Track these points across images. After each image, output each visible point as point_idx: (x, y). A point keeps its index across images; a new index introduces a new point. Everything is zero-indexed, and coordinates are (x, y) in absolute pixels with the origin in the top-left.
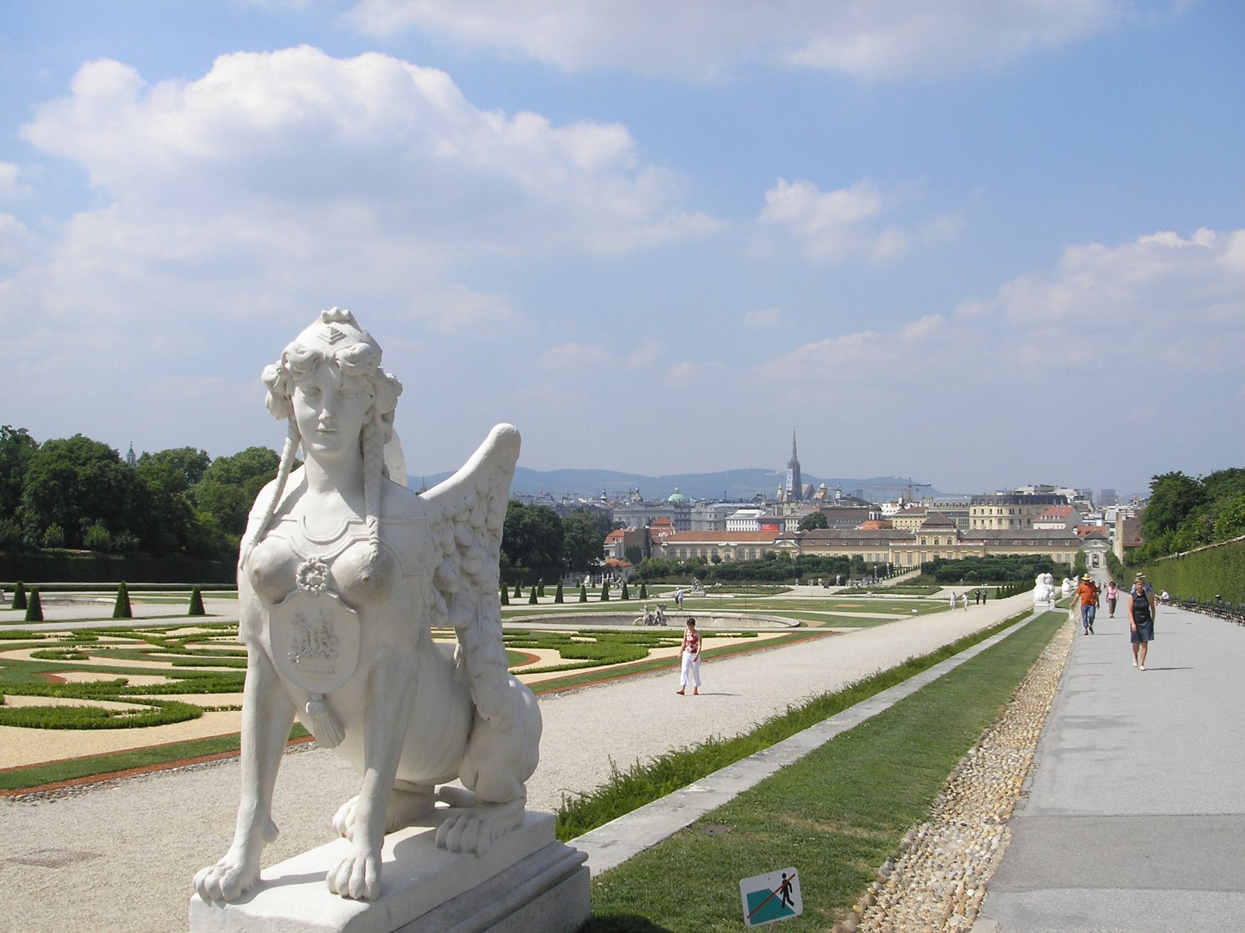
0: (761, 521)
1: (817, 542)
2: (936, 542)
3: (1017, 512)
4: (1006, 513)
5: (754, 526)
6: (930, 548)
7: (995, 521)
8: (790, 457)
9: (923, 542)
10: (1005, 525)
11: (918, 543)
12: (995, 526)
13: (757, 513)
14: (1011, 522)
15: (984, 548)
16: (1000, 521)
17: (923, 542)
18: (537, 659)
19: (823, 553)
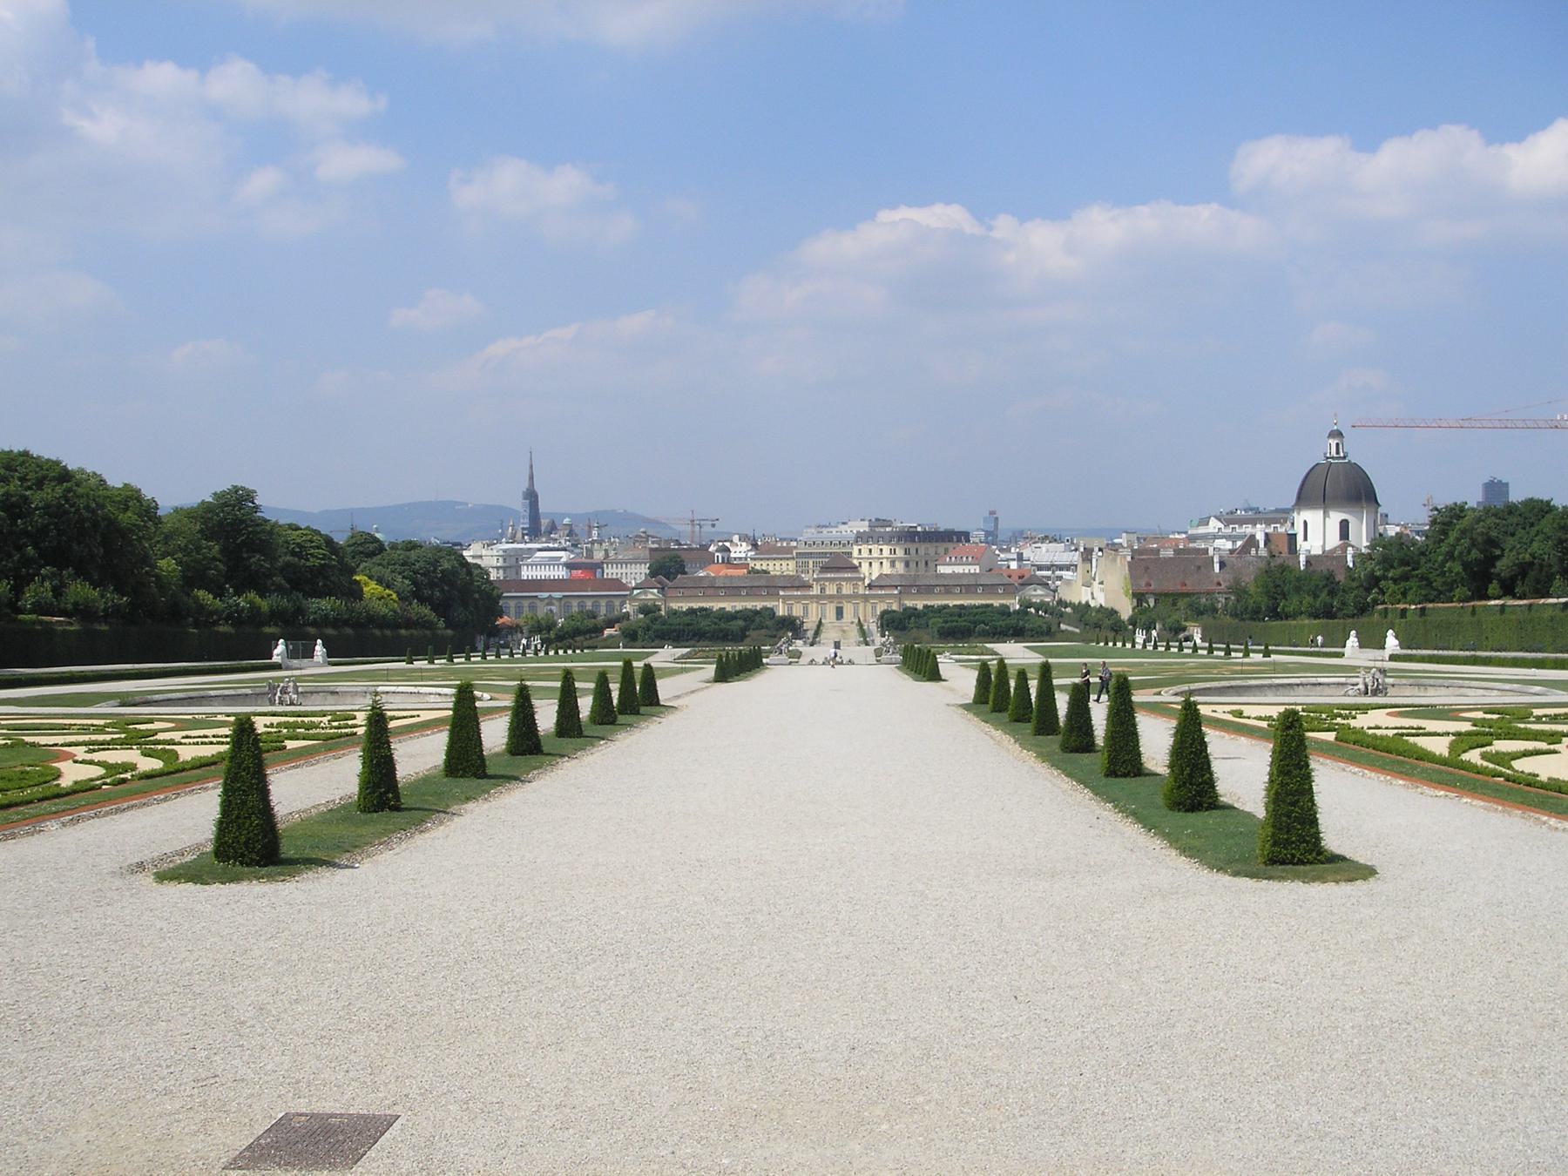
0: (570, 566)
1: (687, 592)
2: (839, 589)
3: (913, 551)
4: (900, 553)
5: (561, 573)
6: (831, 597)
7: (886, 564)
8: (526, 485)
9: (823, 590)
10: (900, 567)
11: (816, 591)
12: (887, 569)
13: (564, 556)
14: (907, 564)
15: (899, 597)
16: (893, 564)
17: (823, 590)
18: (1231, 712)
19: (716, 605)
